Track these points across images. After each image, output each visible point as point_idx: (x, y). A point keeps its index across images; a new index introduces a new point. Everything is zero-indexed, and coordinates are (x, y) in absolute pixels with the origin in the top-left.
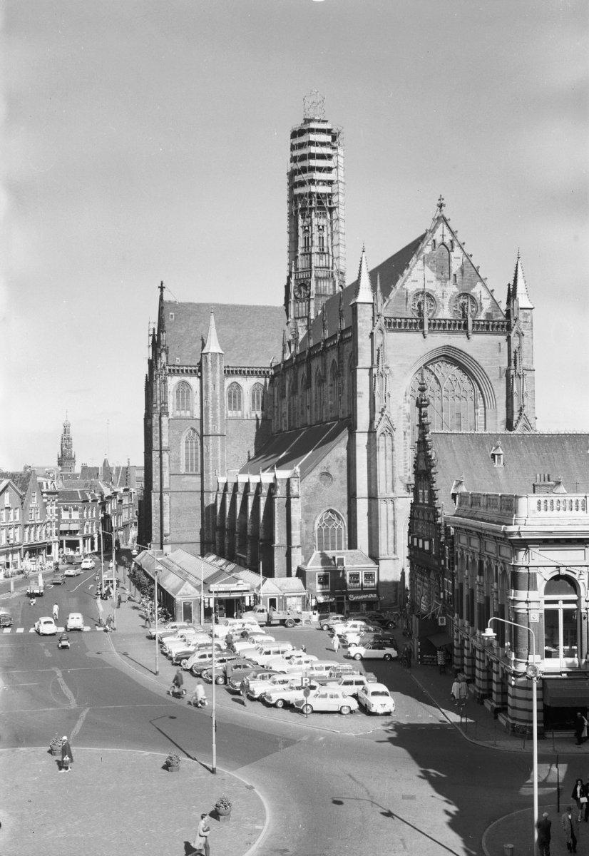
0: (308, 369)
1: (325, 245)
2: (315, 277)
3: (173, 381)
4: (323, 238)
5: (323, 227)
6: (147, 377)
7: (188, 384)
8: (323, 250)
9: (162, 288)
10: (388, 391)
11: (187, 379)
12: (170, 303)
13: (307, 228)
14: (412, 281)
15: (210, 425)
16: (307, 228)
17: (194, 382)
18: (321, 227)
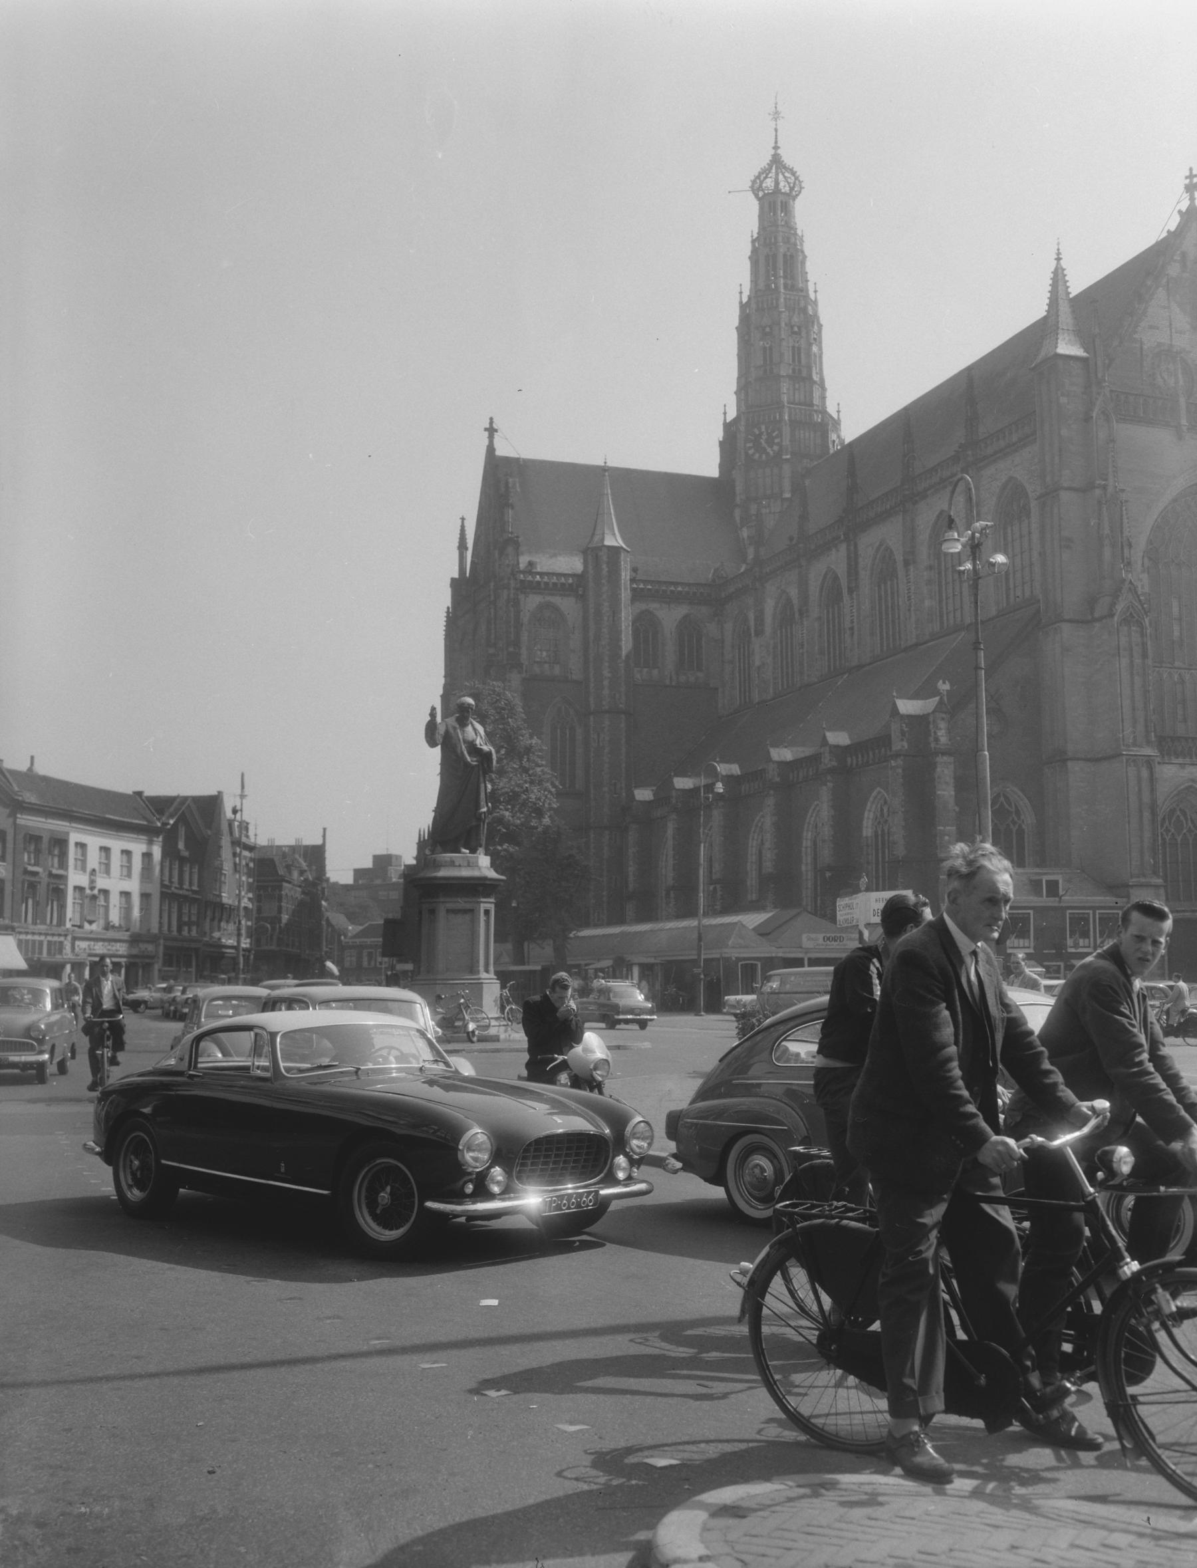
0: (848, 549)
1: (803, 362)
2: (790, 420)
3: (531, 602)
4: (799, 349)
5: (799, 328)
6: (448, 612)
7: (556, 609)
8: (800, 371)
9: (491, 431)
10: (1126, 533)
11: (557, 600)
12: (507, 461)
13: (768, 329)
14: (1151, 327)
15: (606, 692)
16: (768, 329)
17: (567, 605)
18: (796, 329)
